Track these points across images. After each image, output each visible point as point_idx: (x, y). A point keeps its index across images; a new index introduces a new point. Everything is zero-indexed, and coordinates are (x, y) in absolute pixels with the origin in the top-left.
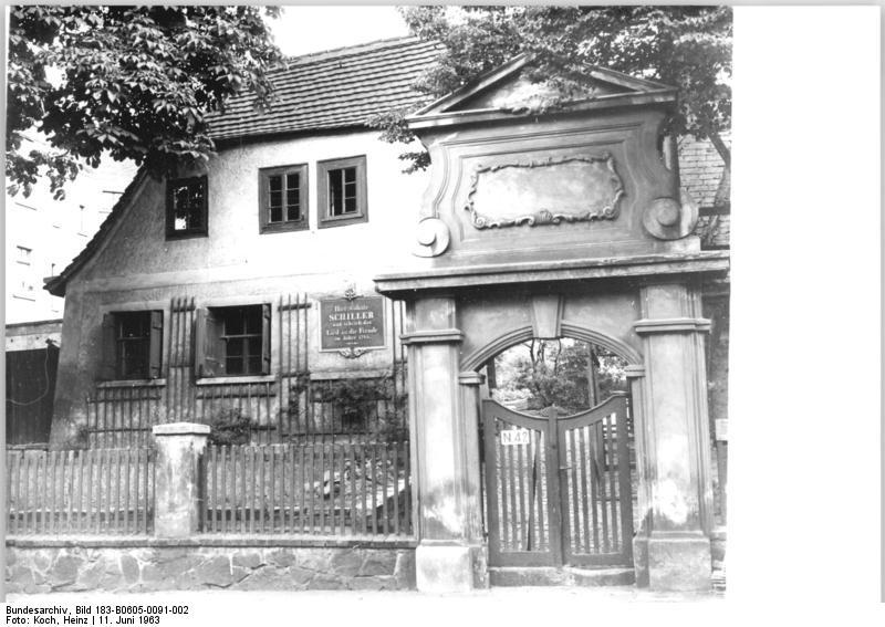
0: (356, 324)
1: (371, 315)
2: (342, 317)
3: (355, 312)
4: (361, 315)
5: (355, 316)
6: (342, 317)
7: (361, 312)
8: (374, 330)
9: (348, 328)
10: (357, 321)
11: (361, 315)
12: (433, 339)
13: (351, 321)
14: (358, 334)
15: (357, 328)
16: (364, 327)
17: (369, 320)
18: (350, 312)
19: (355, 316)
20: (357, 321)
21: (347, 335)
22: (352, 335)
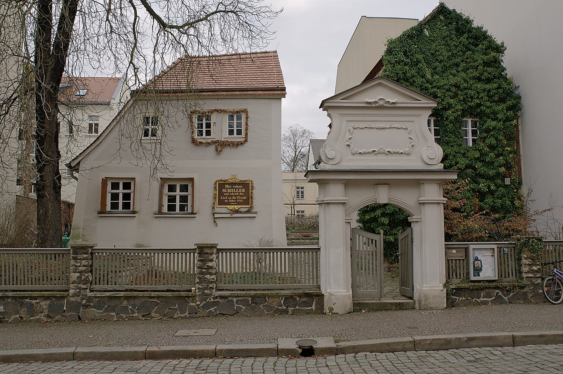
0: (236, 194)
1: (244, 190)
2: (229, 191)
3: (236, 189)
4: (238, 190)
5: (236, 190)
6: (229, 191)
7: (239, 189)
8: (245, 198)
9: (232, 196)
10: (236, 193)
11: (238, 190)
12: (337, 202)
13: (234, 193)
14: (236, 199)
15: (236, 196)
16: (241, 196)
17: (242, 193)
18: (233, 188)
19: (236, 190)
20: (236, 193)
21: (231, 200)
22: (233, 200)
